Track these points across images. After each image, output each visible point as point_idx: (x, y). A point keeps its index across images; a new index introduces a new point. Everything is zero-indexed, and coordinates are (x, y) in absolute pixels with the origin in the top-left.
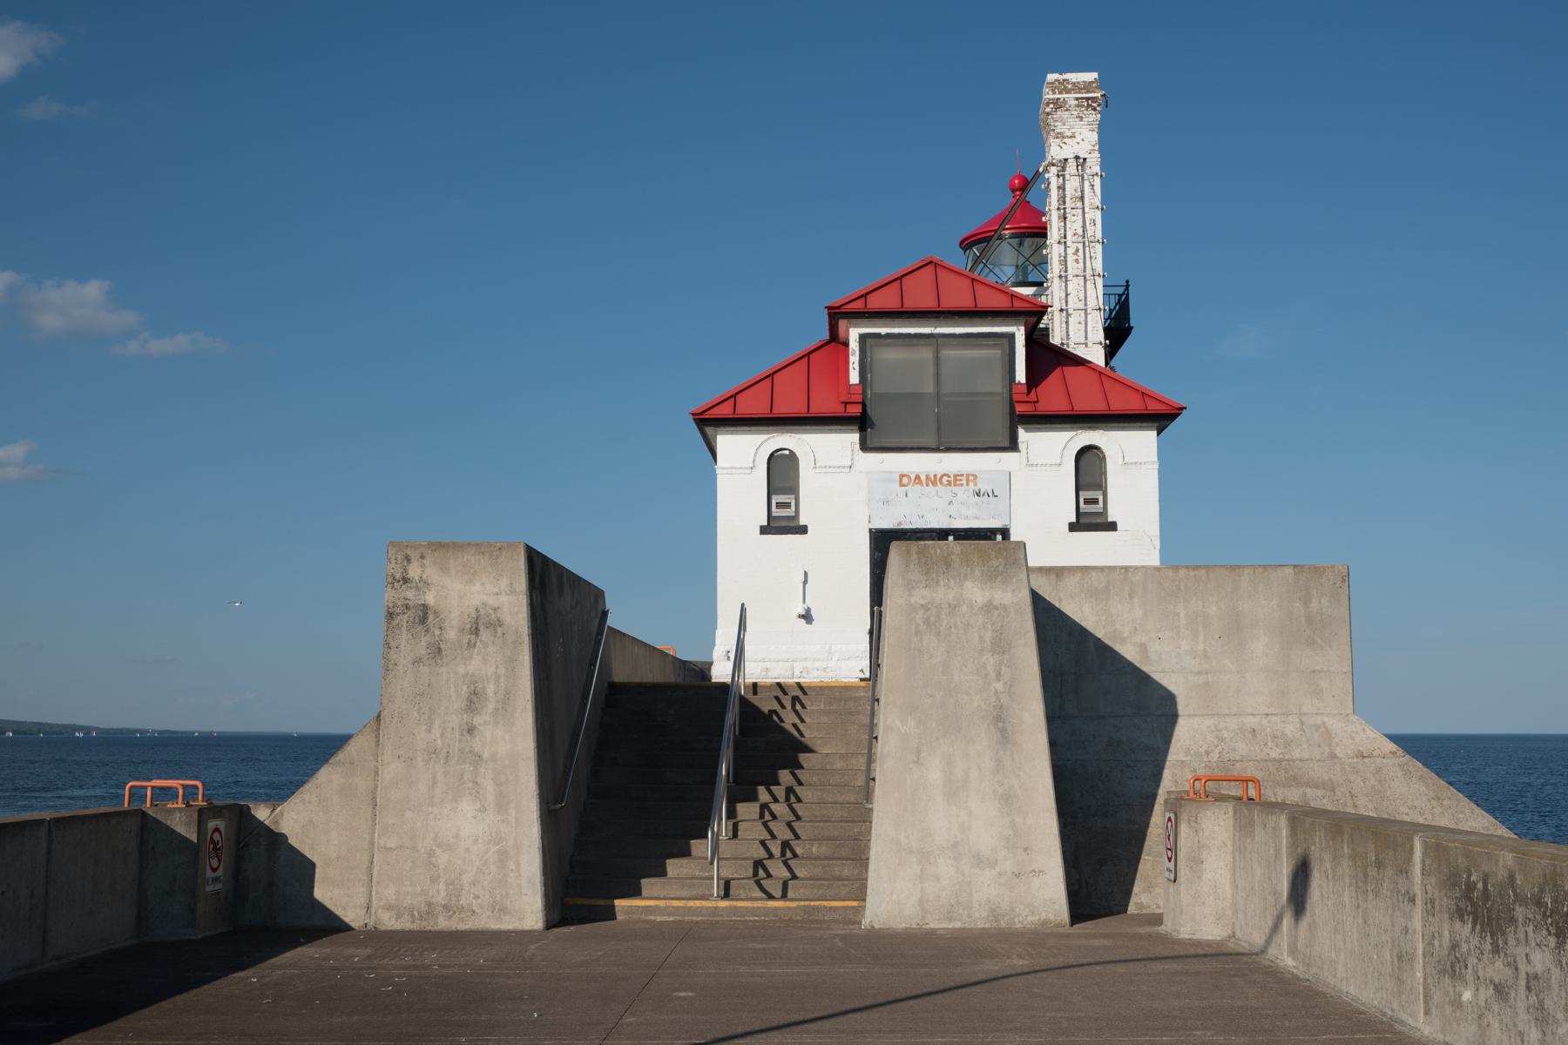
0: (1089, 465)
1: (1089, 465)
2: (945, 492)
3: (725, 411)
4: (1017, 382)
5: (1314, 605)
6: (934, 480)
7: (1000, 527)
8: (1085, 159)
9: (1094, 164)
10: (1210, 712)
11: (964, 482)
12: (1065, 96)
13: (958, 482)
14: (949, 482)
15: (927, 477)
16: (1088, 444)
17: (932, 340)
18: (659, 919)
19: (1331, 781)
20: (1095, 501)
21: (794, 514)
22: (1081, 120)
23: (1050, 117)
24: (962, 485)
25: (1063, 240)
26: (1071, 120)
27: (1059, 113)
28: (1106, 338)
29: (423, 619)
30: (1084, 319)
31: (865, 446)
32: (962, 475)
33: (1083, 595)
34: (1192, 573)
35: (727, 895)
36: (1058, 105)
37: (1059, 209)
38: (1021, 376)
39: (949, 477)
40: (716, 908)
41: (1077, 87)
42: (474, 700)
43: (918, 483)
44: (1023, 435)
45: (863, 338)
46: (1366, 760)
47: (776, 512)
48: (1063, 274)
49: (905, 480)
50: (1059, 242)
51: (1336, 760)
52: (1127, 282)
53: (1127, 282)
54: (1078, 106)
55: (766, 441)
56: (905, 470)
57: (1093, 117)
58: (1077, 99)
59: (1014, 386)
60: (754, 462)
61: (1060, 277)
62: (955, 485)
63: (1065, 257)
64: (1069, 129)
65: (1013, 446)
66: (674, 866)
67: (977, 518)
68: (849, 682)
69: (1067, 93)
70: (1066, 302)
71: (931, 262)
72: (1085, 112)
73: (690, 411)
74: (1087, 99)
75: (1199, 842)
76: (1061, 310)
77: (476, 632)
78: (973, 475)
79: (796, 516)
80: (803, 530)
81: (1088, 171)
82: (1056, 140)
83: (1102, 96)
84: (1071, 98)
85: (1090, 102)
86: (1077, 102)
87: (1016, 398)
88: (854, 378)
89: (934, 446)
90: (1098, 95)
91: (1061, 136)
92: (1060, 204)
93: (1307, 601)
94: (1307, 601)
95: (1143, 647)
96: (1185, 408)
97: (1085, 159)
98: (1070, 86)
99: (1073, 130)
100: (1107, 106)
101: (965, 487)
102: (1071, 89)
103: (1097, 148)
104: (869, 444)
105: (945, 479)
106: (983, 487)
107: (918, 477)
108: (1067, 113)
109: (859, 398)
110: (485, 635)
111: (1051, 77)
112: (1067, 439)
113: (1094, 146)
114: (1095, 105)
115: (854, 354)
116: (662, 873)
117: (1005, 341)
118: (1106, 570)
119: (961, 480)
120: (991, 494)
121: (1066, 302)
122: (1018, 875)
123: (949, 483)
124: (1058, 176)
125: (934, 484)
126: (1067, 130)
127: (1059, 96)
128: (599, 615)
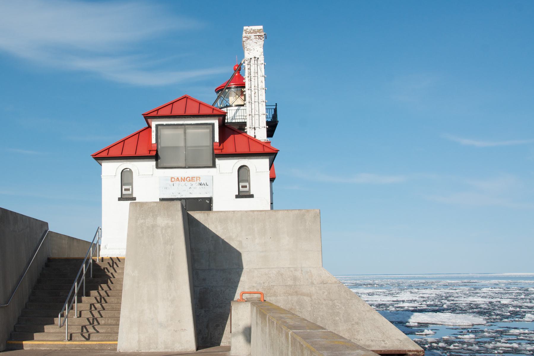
0: (243, 172)
1: (243, 172)
2: (189, 184)
3: (104, 154)
4: (215, 142)
6: (183, 179)
7: (209, 197)
8: (258, 58)
9: (262, 60)
10: (266, 267)
11: (195, 180)
12: (250, 35)
13: (193, 180)
14: (190, 180)
15: (181, 178)
16: (242, 165)
17: (183, 126)
18: (43, 349)
19: (311, 293)
20: (246, 187)
21: (131, 193)
22: (256, 44)
23: (245, 43)
24: (194, 181)
25: (250, 89)
26: (253, 44)
27: (248, 41)
28: (267, 125)
30: (258, 118)
31: (157, 167)
32: (195, 177)
33: (217, 222)
34: (260, 213)
35: (71, 339)
36: (248, 38)
37: (248, 77)
38: (217, 139)
39: (190, 178)
40: (65, 345)
41: (254, 31)
43: (178, 181)
44: (218, 162)
45: (157, 126)
46: (325, 285)
47: (124, 192)
48: (250, 101)
49: (173, 180)
50: (249, 89)
51: (313, 285)
52: (276, 104)
53: (276, 104)
54: (255, 38)
55: (120, 165)
57: (261, 42)
58: (255, 36)
59: (214, 143)
60: (116, 173)
61: (249, 102)
62: (192, 181)
63: (251, 95)
64: (252, 47)
65: (214, 166)
66: (47, 328)
68: (122, 257)
69: (251, 34)
70: (252, 112)
71: (186, 97)
72: (258, 41)
73: (91, 154)
74: (259, 36)
75: (238, 318)
76: (250, 115)
78: (198, 177)
79: (132, 194)
81: (259, 62)
82: (247, 51)
83: (264, 34)
84: (252, 35)
85: (260, 37)
86: (255, 37)
87: (215, 147)
88: (154, 141)
89: (184, 166)
90: (263, 34)
92: (249, 75)
95: (240, 242)
96: (279, 151)
97: (258, 58)
98: (252, 31)
99: (253, 48)
100: (266, 38)
101: (196, 182)
102: (252, 32)
103: (263, 54)
105: (188, 179)
106: (202, 182)
107: (178, 178)
108: (251, 41)
109: (155, 149)
111: (245, 28)
112: (234, 163)
113: (261, 53)
114: (262, 38)
115: (153, 132)
116: (42, 330)
117: (211, 126)
118: (226, 212)
119: (194, 179)
120: (205, 184)
121: (252, 112)
122: (176, 331)
123: (190, 180)
124: (248, 65)
125: (184, 181)
126: (251, 48)
127: (249, 35)
128: (43, 232)
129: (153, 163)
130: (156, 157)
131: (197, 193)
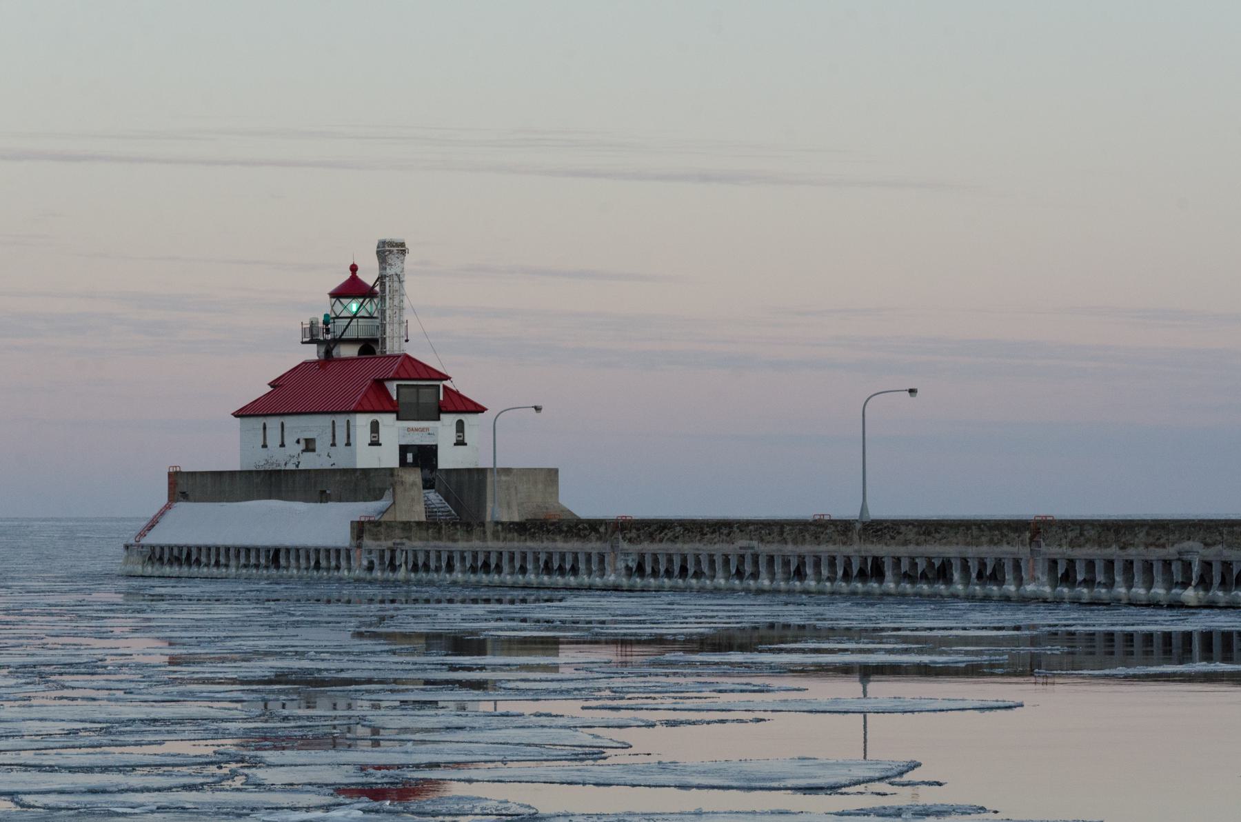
2: (420, 433)
6: (417, 430)
31: (398, 419)
36: (391, 252)
44: (442, 416)
45: (398, 386)
47: (373, 439)
79: (378, 441)
88: (395, 398)
91: (390, 265)
106: (430, 432)
129: (394, 416)
130: (397, 412)
131: (426, 441)
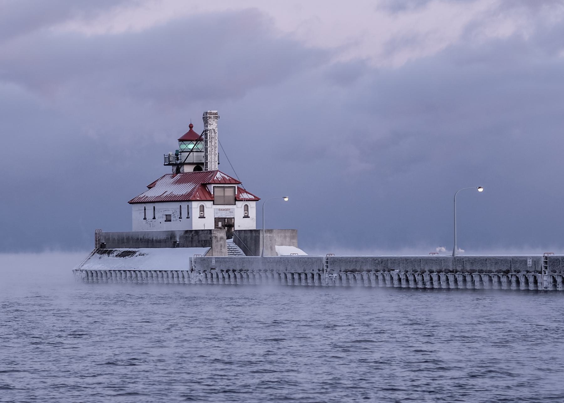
0: (246, 208)
1: (246, 208)
5: (294, 234)
6: (224, 210)
17: (223, 188)
29: (216, 238)
31: (214, 204)
38: (236, 193)
42: (221, 246)
44: (237, 202)
56: (220, 208)
65: (235, 204)
67: (230, 216)
77: (221, 239)
79: (204, 216)
80: (205, 218)
93: (293, 233)
94: (293, 233)
104: (215, 204)
106: (231, 211)
110: (222, 239)
129: (212, 202)
130: (213, 201)
